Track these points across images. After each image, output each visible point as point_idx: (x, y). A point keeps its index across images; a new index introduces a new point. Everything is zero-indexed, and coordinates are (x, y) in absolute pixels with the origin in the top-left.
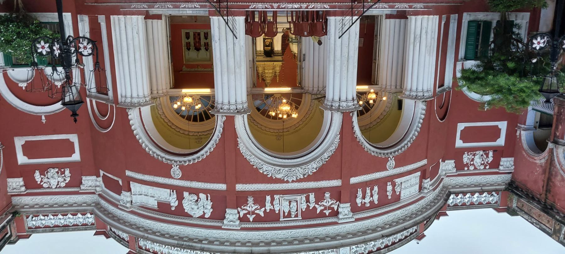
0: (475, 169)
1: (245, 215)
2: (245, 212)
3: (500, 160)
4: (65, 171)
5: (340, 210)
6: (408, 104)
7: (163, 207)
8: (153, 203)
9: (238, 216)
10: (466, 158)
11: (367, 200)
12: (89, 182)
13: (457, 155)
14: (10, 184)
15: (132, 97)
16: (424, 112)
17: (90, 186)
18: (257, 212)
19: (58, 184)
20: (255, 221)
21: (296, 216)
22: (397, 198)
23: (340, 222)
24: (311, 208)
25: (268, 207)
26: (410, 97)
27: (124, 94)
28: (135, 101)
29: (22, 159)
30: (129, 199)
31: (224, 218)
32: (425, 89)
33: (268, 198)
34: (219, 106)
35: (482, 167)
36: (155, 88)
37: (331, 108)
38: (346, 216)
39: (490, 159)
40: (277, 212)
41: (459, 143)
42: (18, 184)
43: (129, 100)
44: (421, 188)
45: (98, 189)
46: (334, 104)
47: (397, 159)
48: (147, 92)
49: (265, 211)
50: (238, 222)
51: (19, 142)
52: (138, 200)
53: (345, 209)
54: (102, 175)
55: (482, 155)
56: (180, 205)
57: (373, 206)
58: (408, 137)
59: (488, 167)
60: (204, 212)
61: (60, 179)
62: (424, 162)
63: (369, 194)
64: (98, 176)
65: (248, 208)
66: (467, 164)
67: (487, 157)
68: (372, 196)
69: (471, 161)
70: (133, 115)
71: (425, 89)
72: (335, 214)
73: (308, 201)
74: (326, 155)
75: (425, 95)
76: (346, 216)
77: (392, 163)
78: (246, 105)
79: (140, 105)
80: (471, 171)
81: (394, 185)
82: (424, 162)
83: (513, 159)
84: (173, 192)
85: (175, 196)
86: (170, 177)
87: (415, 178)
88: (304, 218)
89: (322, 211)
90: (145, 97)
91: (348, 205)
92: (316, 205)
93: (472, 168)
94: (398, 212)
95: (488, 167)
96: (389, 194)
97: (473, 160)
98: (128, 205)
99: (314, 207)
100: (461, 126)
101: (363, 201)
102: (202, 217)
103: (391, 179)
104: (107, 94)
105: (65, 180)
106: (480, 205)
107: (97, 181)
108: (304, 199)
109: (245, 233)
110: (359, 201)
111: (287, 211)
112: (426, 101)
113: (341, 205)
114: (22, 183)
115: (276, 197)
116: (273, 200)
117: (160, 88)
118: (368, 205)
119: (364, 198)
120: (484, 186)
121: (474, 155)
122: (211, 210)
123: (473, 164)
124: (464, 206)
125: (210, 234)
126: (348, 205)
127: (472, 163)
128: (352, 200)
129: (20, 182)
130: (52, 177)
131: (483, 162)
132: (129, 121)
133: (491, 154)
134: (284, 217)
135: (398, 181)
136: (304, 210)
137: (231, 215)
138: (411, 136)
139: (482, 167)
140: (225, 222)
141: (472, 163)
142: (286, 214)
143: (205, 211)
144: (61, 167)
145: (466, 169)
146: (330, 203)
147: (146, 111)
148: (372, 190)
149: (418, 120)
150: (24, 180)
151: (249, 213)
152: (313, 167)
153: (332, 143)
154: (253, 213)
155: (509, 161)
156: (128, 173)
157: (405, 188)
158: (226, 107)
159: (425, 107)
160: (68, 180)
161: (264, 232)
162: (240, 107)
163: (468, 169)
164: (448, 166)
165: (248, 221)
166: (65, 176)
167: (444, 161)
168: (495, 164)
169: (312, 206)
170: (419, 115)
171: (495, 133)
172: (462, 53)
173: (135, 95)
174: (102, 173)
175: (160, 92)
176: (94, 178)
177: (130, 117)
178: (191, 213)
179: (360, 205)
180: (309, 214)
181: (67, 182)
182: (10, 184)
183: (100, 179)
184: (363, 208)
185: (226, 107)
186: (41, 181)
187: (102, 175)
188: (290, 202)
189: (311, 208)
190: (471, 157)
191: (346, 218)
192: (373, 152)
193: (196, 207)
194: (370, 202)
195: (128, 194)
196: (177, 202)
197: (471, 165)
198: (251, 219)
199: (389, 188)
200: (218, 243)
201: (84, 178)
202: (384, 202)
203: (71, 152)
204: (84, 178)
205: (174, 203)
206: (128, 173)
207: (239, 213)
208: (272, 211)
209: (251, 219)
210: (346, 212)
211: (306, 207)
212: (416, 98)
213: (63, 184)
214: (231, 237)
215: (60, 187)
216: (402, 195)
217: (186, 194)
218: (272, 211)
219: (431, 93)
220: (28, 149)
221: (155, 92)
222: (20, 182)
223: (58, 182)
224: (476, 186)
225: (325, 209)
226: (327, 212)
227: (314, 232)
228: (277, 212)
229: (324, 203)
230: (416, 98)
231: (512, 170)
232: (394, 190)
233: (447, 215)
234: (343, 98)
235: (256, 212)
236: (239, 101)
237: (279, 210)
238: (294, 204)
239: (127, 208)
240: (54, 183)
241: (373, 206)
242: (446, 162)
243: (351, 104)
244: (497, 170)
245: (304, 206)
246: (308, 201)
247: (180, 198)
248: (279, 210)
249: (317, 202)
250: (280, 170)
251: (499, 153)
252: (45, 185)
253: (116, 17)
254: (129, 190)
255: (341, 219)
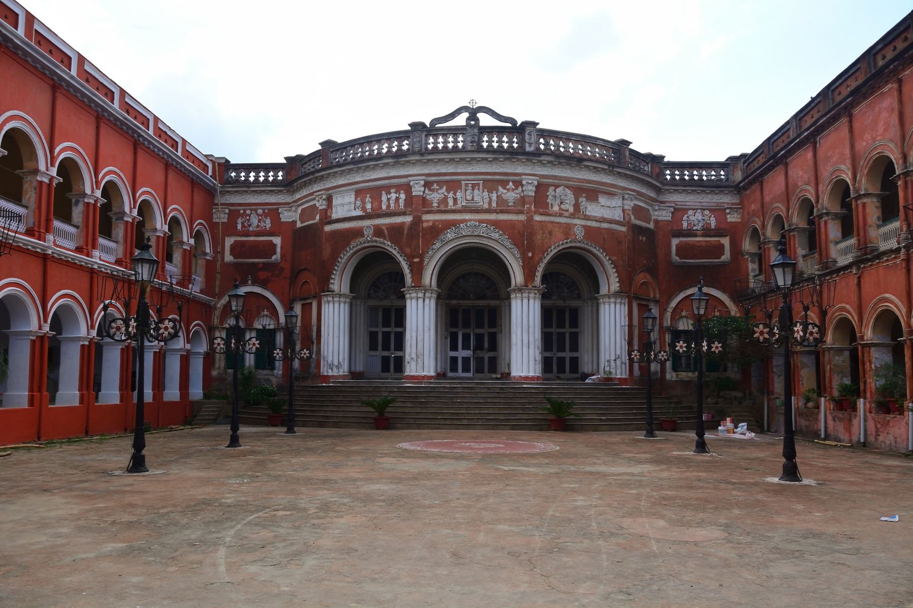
0: (256, 210)
1: (517, 188)
2: (517, 191)
3: (228, 219)
4: (687, 227)
5: (422, 189)
6: (345, 289)
7: (592, 194)
8: (602, 200)
9: (524, 189)
10: (268, 224)
11: (393, 196)
12: (665, 215)
13: (278, 228)
14: (739, 216)
15: (615, 303)
16: (332, 281)
17: (664, 210)
18: (505, 191)
19: (695, 213)
20: (508, 182)
21: (467, 185)
22: (359, 193)
23: (423, 177)
24: (452, 192)
25: (494, 197)
26: (345, 296)
27: (623, 306)
28: (612, 300)
29: (726, 241)
30: (625, 202)
31: (536, 187)
32: (331, 305)
33: (494, 205)
34: (537, 296)
35: (248, 212)
36: (595, 308)
37: (432, 290)
38: (417, 182)
39: (240, 221)
40: (486, 190)
41: (277, 240)
42: (732, 216)
43: (619, 300)
44: (329, 199)
45: (657, 208)
46: (430, 295)
47: (362, 235)
48: (602, 307)
49: (497, 191)
50: (524, 182)
51: (726, 256)
52: (616, 202)
53: (418, 190)
54: (652, 223)
55: (250, 226)
56: (577, 199)
57: (388, 189)
58: (348, 257)
59: (242, 212)
60: (555, 192)
61: (692, 218)
62: (328, 228)
63: (391, 202)
64: (657, 222)
65: (514, 195)
66: (266, 217)
67: (242, 223)
68: (388, 200)
69: (261, 219)
70: (615, 286)
71: (331, 305)
72: (427, 185)
73: (455, 200)
74: (438, 245)
75: (331, 299)
76: (417, 182)
77: (368, 233)
78: (513, 296)
79: (609, 297)
80: (261, 209)
81: (364, 209)
82: (328, 228)
83: (214, 221)
84: (583, 212)
85: (582, 208)
86: (584, 226)
87: (338, 212)
88: (459, 181)
89: (441, 188)
90: (604, 302)
91: (414, 194)
92: (446, 194)
93: (260, 211)
94: (358, 179)
95: (242, 212)
96: (368, 199)
97: (259, 221)
98: (627, 196)
99: (449, 193)
100: (277, 257)
101: (397, 196)
102: (557, 186)
103: (367, 216)
104: (639, 305)
105: (688, 217)
106: (249, 167)
107: (658, 216)
108: (459, 202)
109: (517, 171)
110: (403, 196)
111: (476, 191)
112: (331, 291)
113: (422, 194)
114: (728, 216)
115: (486, 206)
116: (490, 203)
117: (590, 308)
118: (393, 190)
119: (397, 199)
120: (246, 191)
121: (258, 226)
122: (548, 194)
123: (258, 215)
124: (267, 167)
125: (550, 170)
126: (414, 194)
127: (260, 218)
128: (410, 199)
129: (730, 218)
130: (699, 221)
131: (248, 218)
132: (618, 282)
133: (239, 227)
134: (478, 184)
135: (359, 213)
136: (459, 191)
137: (530, 191)
138: (346, 258)
139: (248, 212)
140: (536, 183)
141: (260, 218)
142: (477, 187)
143: (553, 193)
144: (690, 233)
145: (266, 211)
146: (432, 196)
147: (604, 290)
148: (388, 206)
149: (338, 273)
150: (727, 219)
151: (513, 190)
152: (450, 235)
153: (432, 257)
154: (508, 190)
155: (218, 218)
156: (624, 229)
157: (350, 203)
158: (532, 295)
159: (331, 286)
160: (685, 218)
161: (499, 171)
162: (519, 295)
163: (264, 210)
164: (287, 216)
165: (514, 182)
166: (688, 221)
167: (294, 222)
168: (234, 215)
169: (451, 195)
170: (337, 278)
171: (236, 249)
172: (280, 338)
173: (612, 305)
174: (651, 226)
175: (590, 304)
176: (660, 218)
177: (618, 285)
178: (568, 191)
179: (402, 192)
180: (453, 186)
181: (686, 216)
182: (739, 216)
183: (653, 218)
184: (398, 188)
185: (532, 295)
186: (710, 217)
187: (652, 223)
188: (473, 199)
189: (452, 192)
190: (262, 224)
191: (417, 180)
192: (388, 245)
193: (562, 197)
194: (390, 193)
195: (626, 207)
196: (580, 201)
197: (261, 215)
198: (511, 183)
199: (369, 206)
200: (544, 162)
201: (670, 218)
202: (376, 192)
203: (679, 248)
204: (670, 218)
205: (582, 200)
206: (624, 229)
207: (523, 191)
208: (490, 192)
209: (511, 183)
210: (417, 186)
211: (457, 194)
212: (340, 296)
213: (690, 212)
214: (530, 168)
215: (693, 210)
216: (353, 196)
217: (571, 209)
218: (490, 192)
219: (324, 299)
220: (720, 248)
221: (595, 304)
222: (730, 218)
223: (694, 216)
224: (255, 191)
225: (437, 190)
226: (435, 186)
227: (450, 168)
228: (486, 190)
229: (438, 196)
230: (340, 296)
231: (215, 208)
232: (364, 203)
233: (285, 158)
234: (421, 301)
235: (506, 191)
236: (519, 301)
237: (483, 192)
238: (469, 198)
239: (628, 194)
240: (699, 216)
241: (388, 189)
242: (291, 220)
243: (414, 295)
244: (231, 208)
245: (459, 195)
246: (455, 200)
247: (577, 206)
248: (483, 192)
249: (446, 198)
250: (483, 233)
251: (230, 228)
252: (707, 212)
253: (624, 377)
254: (624, 211)
255: (422, 180)
